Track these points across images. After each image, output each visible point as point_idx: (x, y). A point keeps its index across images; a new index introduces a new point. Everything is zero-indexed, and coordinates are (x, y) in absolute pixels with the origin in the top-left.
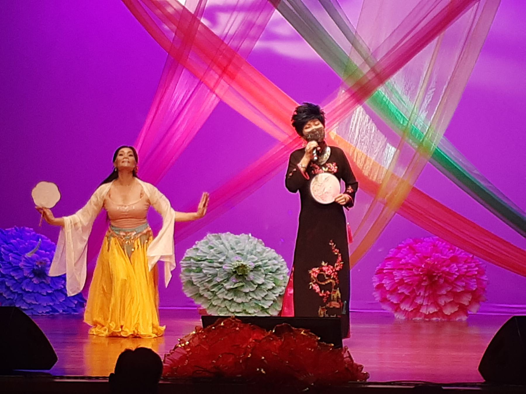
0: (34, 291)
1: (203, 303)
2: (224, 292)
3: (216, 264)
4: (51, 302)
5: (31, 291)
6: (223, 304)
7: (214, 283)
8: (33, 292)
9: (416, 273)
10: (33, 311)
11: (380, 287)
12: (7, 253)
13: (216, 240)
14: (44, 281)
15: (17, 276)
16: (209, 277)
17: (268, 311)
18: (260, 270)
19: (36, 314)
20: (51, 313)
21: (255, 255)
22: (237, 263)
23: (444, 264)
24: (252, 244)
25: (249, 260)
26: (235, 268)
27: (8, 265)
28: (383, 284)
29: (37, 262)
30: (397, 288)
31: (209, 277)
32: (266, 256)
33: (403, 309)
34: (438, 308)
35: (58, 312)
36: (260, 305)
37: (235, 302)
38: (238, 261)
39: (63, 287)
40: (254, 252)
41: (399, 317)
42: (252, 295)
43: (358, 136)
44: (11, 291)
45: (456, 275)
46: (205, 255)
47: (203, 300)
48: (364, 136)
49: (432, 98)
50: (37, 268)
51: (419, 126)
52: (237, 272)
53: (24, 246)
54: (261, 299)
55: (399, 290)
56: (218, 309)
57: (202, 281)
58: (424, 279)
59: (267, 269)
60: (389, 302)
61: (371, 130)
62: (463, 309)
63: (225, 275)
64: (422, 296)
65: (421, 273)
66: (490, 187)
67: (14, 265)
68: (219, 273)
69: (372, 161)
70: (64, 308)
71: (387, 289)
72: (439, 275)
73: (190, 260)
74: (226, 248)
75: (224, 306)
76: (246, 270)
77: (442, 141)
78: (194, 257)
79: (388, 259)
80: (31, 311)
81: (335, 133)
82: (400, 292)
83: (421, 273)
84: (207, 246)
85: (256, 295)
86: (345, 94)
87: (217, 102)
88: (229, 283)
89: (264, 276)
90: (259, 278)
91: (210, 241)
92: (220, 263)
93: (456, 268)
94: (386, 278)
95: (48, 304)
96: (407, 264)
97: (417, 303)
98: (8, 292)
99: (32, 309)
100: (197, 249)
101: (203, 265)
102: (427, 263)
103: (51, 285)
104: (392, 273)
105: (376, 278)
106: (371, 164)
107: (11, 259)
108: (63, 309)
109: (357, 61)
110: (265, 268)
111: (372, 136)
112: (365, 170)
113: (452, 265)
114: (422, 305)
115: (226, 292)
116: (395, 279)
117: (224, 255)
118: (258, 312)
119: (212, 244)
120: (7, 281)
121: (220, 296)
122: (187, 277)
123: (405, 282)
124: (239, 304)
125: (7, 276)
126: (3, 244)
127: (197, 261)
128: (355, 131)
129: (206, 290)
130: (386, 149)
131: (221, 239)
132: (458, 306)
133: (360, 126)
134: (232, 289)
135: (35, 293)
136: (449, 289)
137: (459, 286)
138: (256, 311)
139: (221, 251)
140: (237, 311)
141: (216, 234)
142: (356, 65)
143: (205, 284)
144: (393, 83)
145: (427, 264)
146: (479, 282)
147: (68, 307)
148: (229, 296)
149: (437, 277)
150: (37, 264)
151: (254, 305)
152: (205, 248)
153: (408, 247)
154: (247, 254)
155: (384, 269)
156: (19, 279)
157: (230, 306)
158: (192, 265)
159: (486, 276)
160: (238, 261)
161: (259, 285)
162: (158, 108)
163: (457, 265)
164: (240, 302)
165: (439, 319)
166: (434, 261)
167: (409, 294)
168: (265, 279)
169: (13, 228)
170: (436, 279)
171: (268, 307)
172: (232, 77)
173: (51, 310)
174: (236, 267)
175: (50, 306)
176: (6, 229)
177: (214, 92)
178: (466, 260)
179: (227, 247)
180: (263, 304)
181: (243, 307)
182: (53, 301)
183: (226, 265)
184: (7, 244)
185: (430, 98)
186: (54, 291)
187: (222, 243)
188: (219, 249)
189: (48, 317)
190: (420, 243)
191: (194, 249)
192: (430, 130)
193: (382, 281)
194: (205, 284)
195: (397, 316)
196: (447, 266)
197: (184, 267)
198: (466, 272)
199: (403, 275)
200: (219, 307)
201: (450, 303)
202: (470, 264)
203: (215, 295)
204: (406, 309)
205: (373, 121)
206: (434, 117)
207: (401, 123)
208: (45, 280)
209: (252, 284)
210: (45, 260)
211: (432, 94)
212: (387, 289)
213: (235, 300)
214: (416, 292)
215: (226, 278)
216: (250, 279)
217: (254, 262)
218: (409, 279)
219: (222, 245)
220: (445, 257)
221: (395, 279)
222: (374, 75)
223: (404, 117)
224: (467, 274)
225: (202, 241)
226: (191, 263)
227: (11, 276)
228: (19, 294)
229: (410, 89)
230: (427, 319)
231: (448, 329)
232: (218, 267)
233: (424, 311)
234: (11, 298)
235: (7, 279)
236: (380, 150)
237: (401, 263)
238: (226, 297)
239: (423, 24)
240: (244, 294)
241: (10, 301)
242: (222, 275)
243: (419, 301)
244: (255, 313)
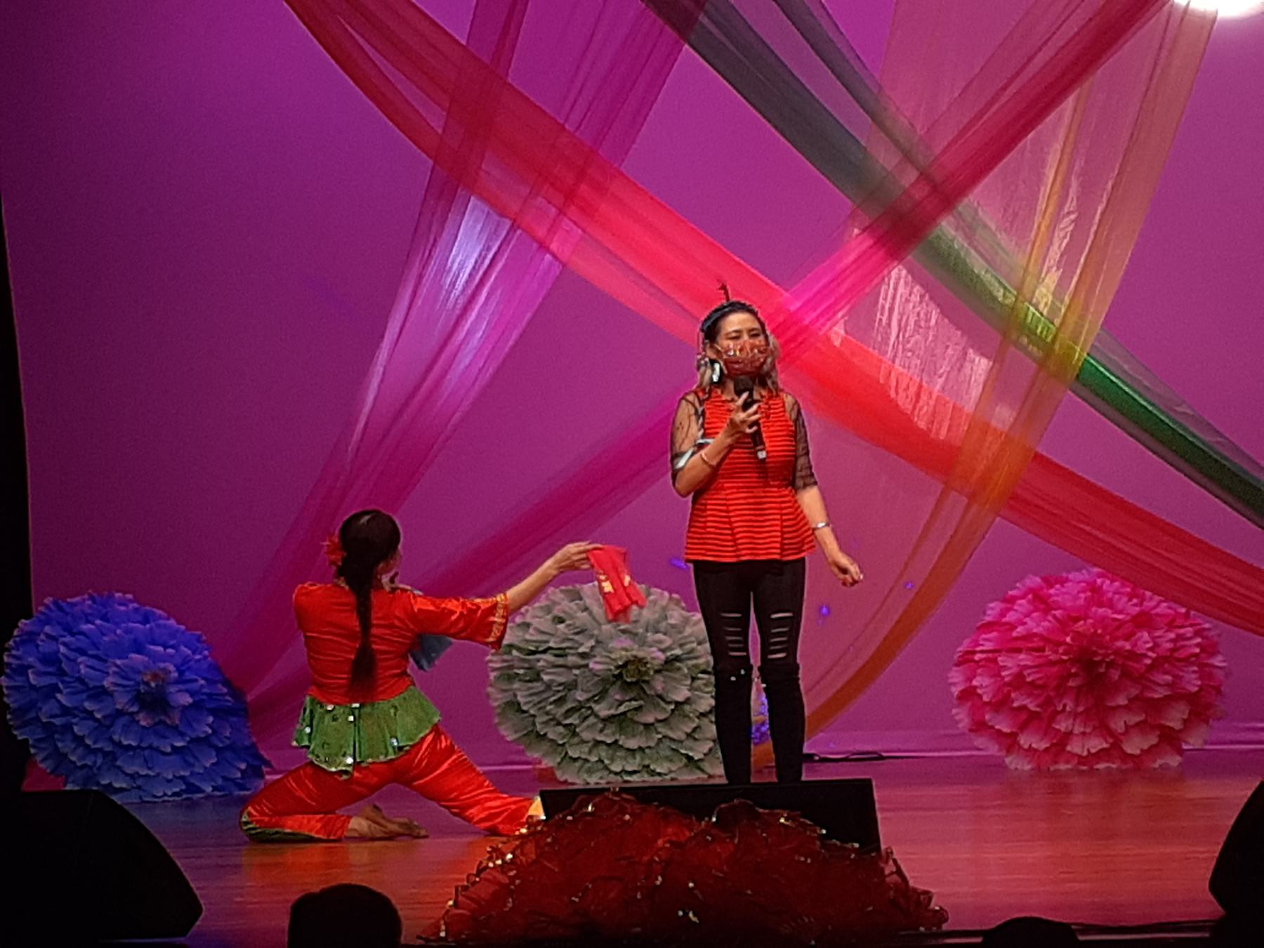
0: (143, 745)
1: (545, 755)
2: (594, 724)
3: (572, 659)
4: (184, 769)
5: (134, 744)
6: (595, 752)
7: (569, 705)
8: (139, 747)
9: (1053, 657)
10: (142, 793)
11: (969, 694)
12: (72, 655)
13: (573, 600)
14: (163, 718)
15: (99, 711)
16: (559, 691)
17: (701, 764)
18: (679, 669)
19: (146, 799)
20: (185, 796)
21: (665, 634)
22: (623, 653)
23: (1120, 633)
24: (657, 608)
25: (651, 646)
26: (618, 667)
27: (76, 684)
28: (975, 687)
29: (146, 674)
30: (1009, 693)
31: (559, 691)
32: (690, 636)
33: (1026, 747)
34: (1111, 741)
35: (202, 791)
36: (683, 751)
37: (621, 746)
38: (626, 650)
39: (210, 731)
40: (663, 625)
41: (1018, 764)
42: (663, 730)
43: (898, 336)
44: (87, 746)
45: (1150, 657)
46: (544, 638)
47: (545, 746)
48: (912, 336)
49: (1071, 236)
50: (146, 688)
51: (1041, 307)
52: (625, 677)
53: (112, 636)
54: (683, 737)
55: (1013, 702)
56: (582, 767)
57: (539, 702)
58: (1073, 671)
59: (696, 666)
60: (992, 730)
61: (928, 320)
62: (1170, 739)
63: (593, 685)
64: (1070, 712)
65: (1065, 658)
66: (1218, 443)
67: (91, 684)
68: (580, 679)
69: (934, 397)
70: (213, 780)
71: (986, 699)
72: (1107, 660)
73: (510, 653)
74: (594, 618)
75: (596, 759)
76: (644, 669)
77: (1098, 338)
78: (522, 645)
79: (988, 627)
80: (134, 792)
81: (842, 332)
82: (1015, 705)
83: (1065, 658)
84: (549, 617)
85: (671, 729)
86: (861, 237)
87: (557, 269)
88: (603, 705)
89: (689, 682)
90: (676, 688)
91: (555, 603)
92: (583, 656)
93: (1147, 642)
94: (980, 675)
95: (177, 775)
96: (1029, 637)
97: (1059, 731)
98: (80, 751)
99: (139, 788)
100: (528, 625)
101: (541, 663)
102: (1078, 632)
103: (182, 729)
104: (995, 661)
105: (957, 674)
106: (932, 403)
107: (83, 670)
108: (213, 784)
109: (884, 159)
110: (691, 663)
111: (931, 333)
112: (918, 416)
113: (1139, 634)
114: (1071, 733)
115: (601, 725)
116: (1003, 674)
117: (592, 636)
118: (679, 769)
119: (564, 612)
120: (76, 724)
121: (586, 735)
122: (507, 694)
123: (1029, 679)
124: (632, 752)
125: (76, 712)
126: (65, 636)
127: (529, 654)
128: (889, 325)
129: (553, 723)
130: (967, 364)
131: (581, 599)
132: (1158, 733)
133: (901, 315)
134: (614, 716)
135: (143, 749)
136: (1134, 692)
137: (1159, 685)
138: (674, 769)
139: (585, 628)
140: (629, 768)
141: (570, 587)
142: (883, 168)
143: (549, 708)
144: (976, 204)
145: (1078, 636)
146: (1206, 672)
147: (225, 779)
148: (606, 735)
149: (1104, 665)
150: (145, 680)
151: (668, 753)
152: (544, 623)
153: (1030, 596)
154: (647, 631)
155: (974, 653)
156: (104, 717)
157: (612, 760)
158: (516, 663)
159: (1220, 658)
160: (626, 650)
161: (678, 704)
162: (420, 277)
163: (1149, 633)
164: (636, 747)
165: (1114, 766)
166: (1093, 625)
167: (1038, 709)
168: (691, 689)
169: (86, 596)
170: (1102, 670)
171: (701, 756)
172: (587, 210)
173: (184, 787)
174: (620, 663)
175: (182, 778)
176: (69, 600)
177: (548, 250)
178: (1173, 620)
179: (597, 617)
180: (691, 749)
181: (642, 759)
182: (189, 765)
183: (597, 659)
184: (73, 635)
185: (1065, 237)
186: (189, 742)
187: (586, 609)
188: (577, 624)
189: (179, 805)
190: (1058, 586)
191: (519, 625)
192: (1069, 314)
193: (971, 681)
194: (549, 708)
195: (1011, 763)
196: (1127, 638)
197: (494, 670)
198: (1173, 650)
199: (1022, 663)
200: (586, 761)
201: (1137, 724)
202: (1182, 631)
203: (574, 734)
204: (1034, 746)
205: (931, 298)
206: (1078, 283)
207: (1000, 299)
208: (166, 714)
209: (663, 704)
210: (164, 670)
211: (1071, 228)
212: (986, 699)
213: (620, 743)
214: (1056, 701)
215: (597, 692)
216: (656, 690)
217: (663, 651)
218: (1037, 672)
219: (585, 614)
220: (1120, 617)
221: (1003, 674)
222: (927, 190)
223: (1005, 288)
224: (1176, 655)
225: (537, 605)
226: (512, 660)
227: (85, 711)
228: (106, 754)
229: (1016, 215)
230: (1084, 768)
231: (1138, 790)
232: (579, 667)
233: (1075, 747)
234: (89, 763)
235: (74, 721)
236: (952, 368)
237: (1014, 634)
238: (599, 738)
239: (1039, 60)
240: (642, 728)
241: (85, 770)
242: (589, 684)
243: (1062, 725)
244: (671, 772)
